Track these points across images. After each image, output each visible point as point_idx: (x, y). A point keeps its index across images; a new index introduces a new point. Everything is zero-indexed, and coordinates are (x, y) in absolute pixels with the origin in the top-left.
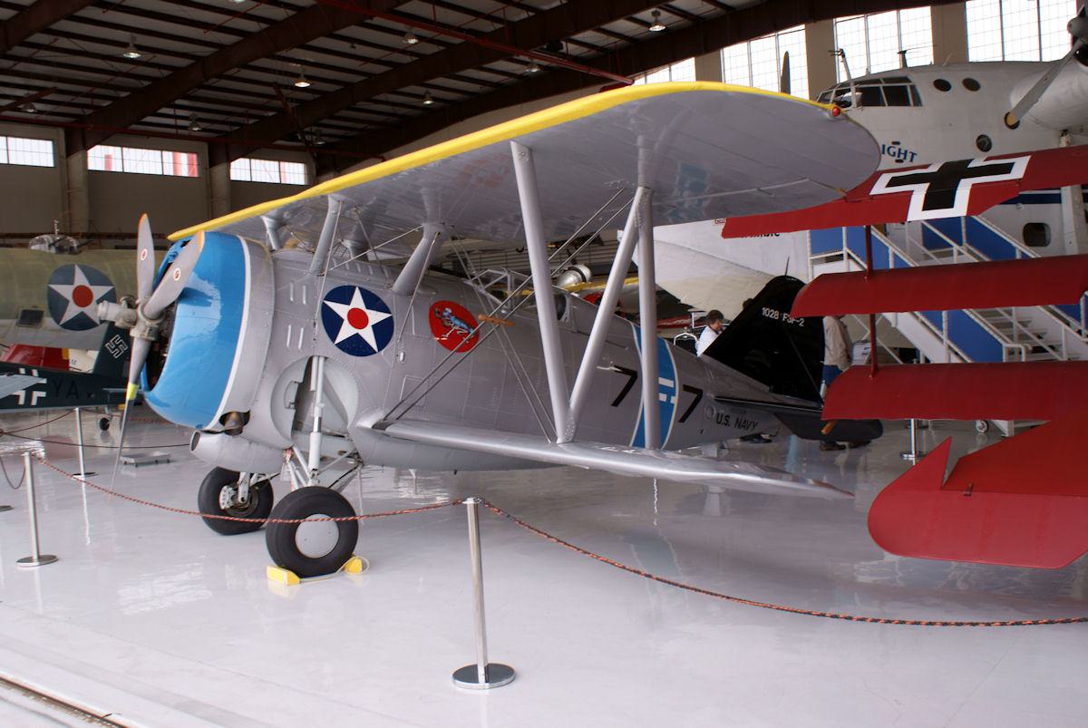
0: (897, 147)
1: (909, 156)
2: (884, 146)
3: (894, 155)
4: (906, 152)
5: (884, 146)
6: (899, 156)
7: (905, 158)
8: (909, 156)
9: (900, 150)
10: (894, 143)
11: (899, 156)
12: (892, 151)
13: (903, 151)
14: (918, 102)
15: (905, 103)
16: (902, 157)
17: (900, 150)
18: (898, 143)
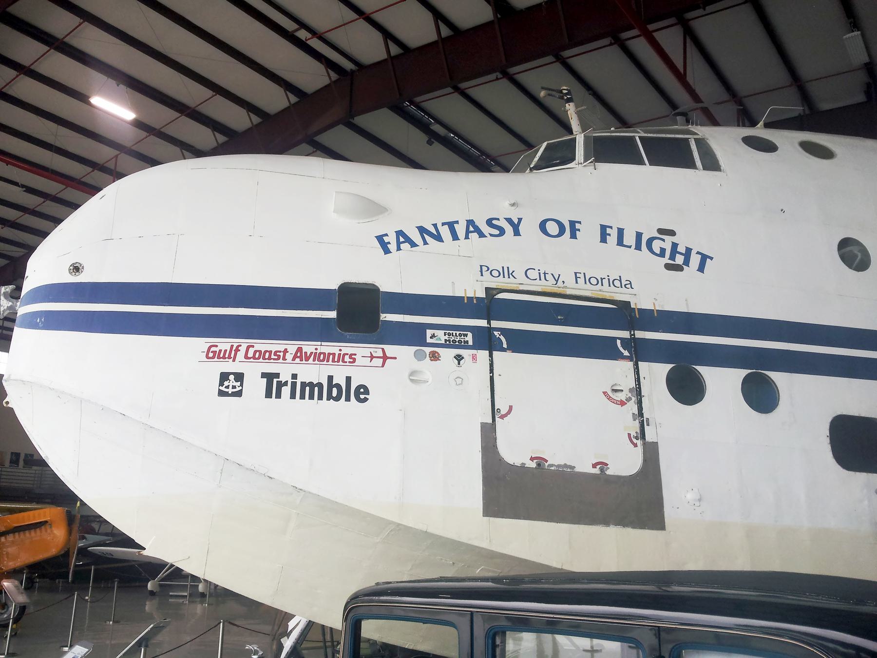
0: (669, 239)
1: (695, 260)
2: (639, 236)
3: (662, 253)
4: (689, 251)
5: (639, 236)
6: (672, 257)
7: (687, 262)
8: (695, 260)
9: (675, 246)
10: (661, 231)
11: (672, 257)
12: (657, 246)
13: (681, 249)
14: (712, 164)
15: (689, 164)
16: (679, 260)
17: (675, 246)
18: (672, 233)
